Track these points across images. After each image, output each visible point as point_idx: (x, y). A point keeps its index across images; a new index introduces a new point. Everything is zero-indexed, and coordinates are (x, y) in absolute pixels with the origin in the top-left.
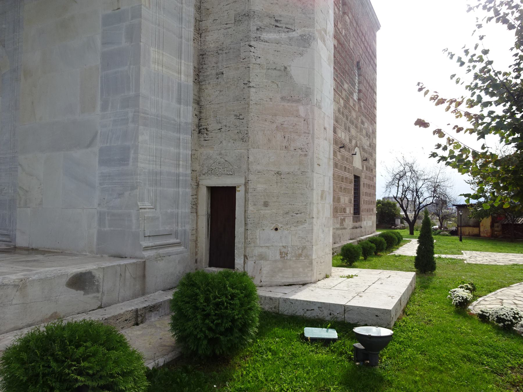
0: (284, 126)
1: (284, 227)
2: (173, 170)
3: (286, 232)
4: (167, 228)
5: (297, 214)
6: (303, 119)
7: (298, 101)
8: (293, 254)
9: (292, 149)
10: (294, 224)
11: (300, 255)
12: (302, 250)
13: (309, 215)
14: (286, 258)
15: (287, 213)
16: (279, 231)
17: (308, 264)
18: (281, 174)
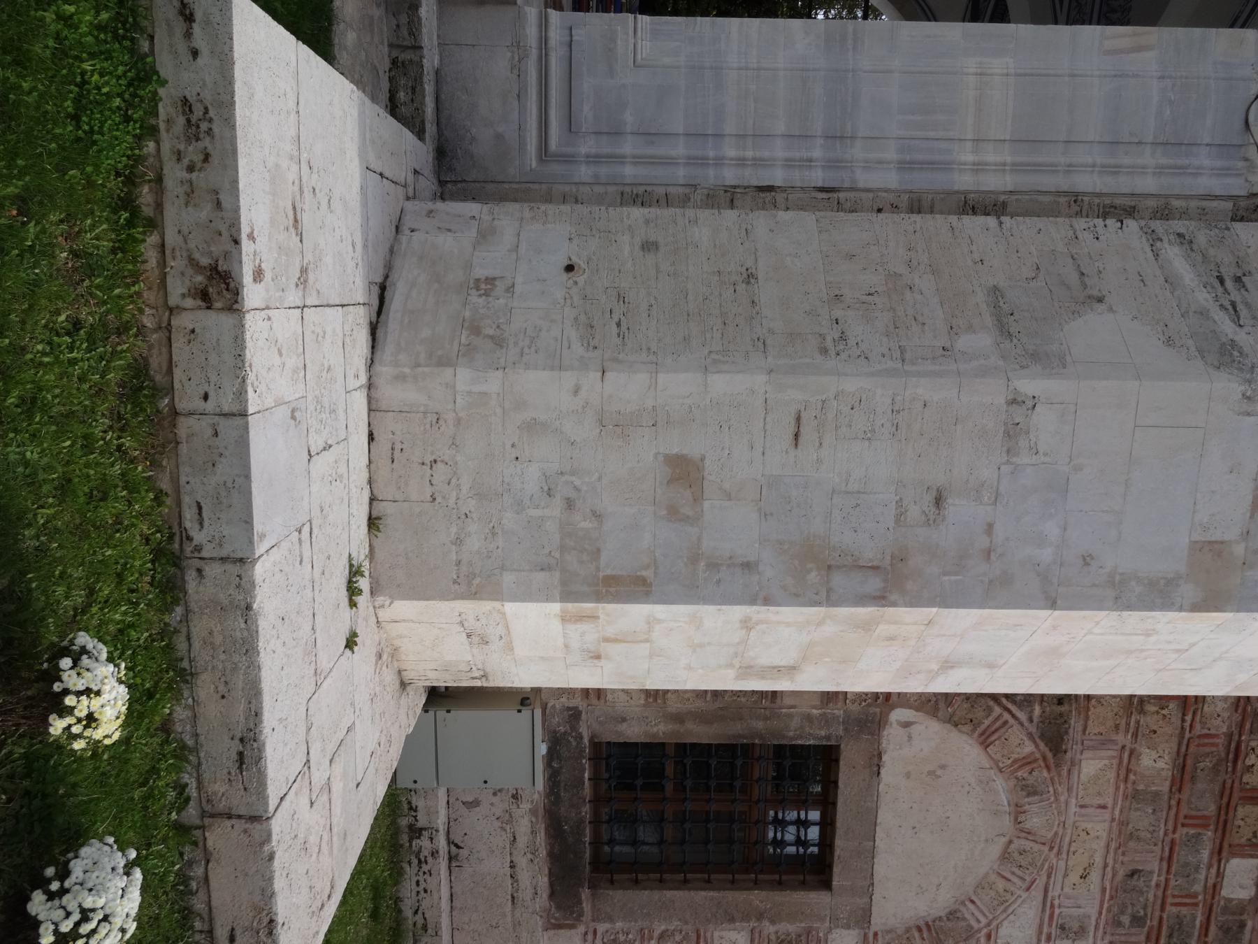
0: (908, 292)
1: (574, 290)
2: (730, 128)
3: (559, 294)
4: (586, 108)
5: (619, 325)
6: (948, 345)
7: (1004, 331)
8: (482, 311)
9: (838, 313)
10: (583, 318)
11: (476, 330)
12: (492, 337)
13: (616, 360)
14: (474, 292)
15: (621, 298)
16: (565, 276)
17: (440, 353)
18: (748, 283)
